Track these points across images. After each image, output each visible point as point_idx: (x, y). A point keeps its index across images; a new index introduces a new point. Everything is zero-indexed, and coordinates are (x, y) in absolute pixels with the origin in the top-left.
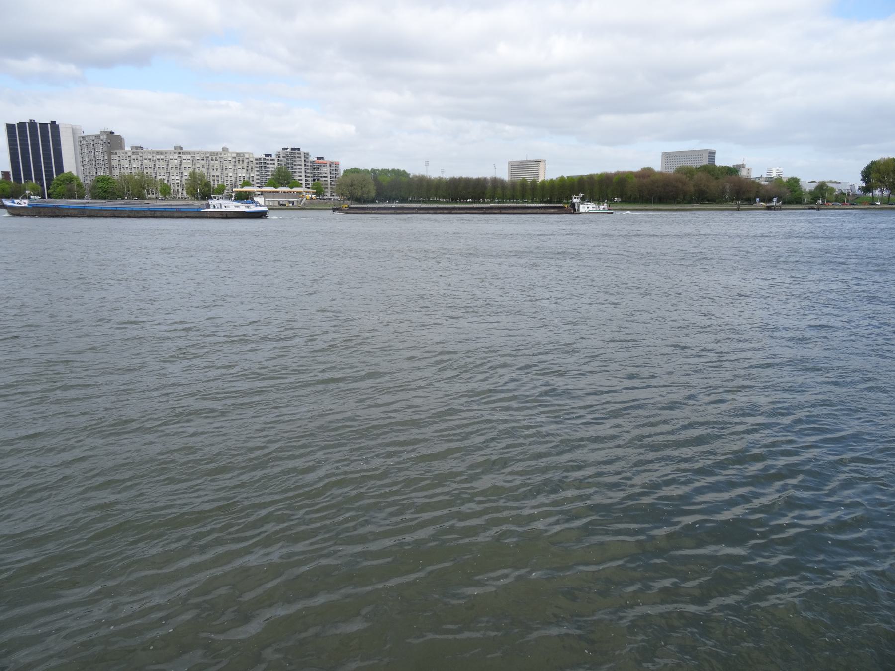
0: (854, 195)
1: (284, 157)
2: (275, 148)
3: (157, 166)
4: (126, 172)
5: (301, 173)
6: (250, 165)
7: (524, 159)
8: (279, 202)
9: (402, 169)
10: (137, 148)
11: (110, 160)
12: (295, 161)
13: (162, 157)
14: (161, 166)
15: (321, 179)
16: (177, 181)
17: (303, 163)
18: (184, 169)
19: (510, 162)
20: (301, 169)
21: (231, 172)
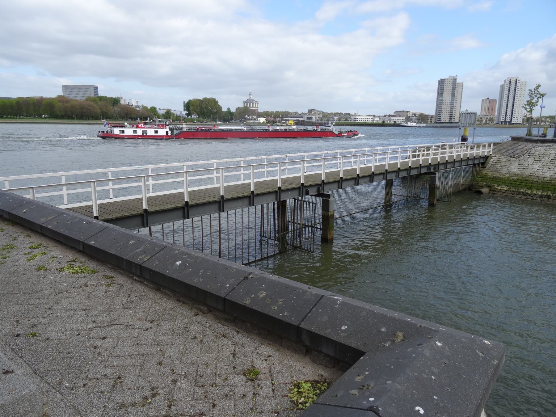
0: (183, 117)
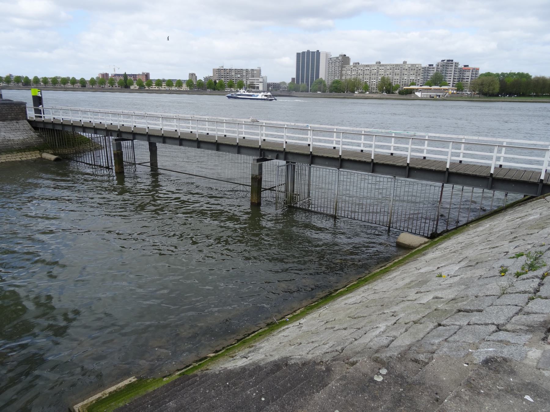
1: (441, 66)
2: (436, 60)
4: (348, 77)
5: (451, 76)
6: (419, 72)
8: (430, 95)
9: (525, 72)
10: (356, 63)
11: (342, 70)
13: (368, 68)
16: (374, 82)
17: (453, 70)
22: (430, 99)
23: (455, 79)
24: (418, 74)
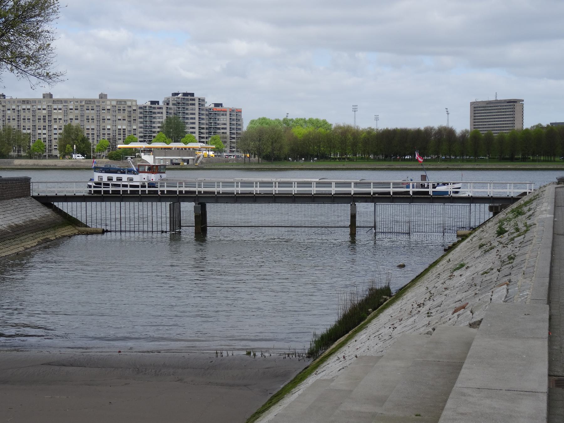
1: (174, 104)
3: (22, 117)
5: (194, 123)
6: (133, 115)
7: (492, 98)
8: (171, 160)
9: (321, 118)
12: (187, 109)
13: (29, 107)
14: (26, 118)
15: (218, 131)
17: (197, 112)
18: (53, 121)
19: (472, 104)
20: (194, 118)
21: (110, 124)
22: (173, 167)
23: (203, 128)
24: (132, 118)
